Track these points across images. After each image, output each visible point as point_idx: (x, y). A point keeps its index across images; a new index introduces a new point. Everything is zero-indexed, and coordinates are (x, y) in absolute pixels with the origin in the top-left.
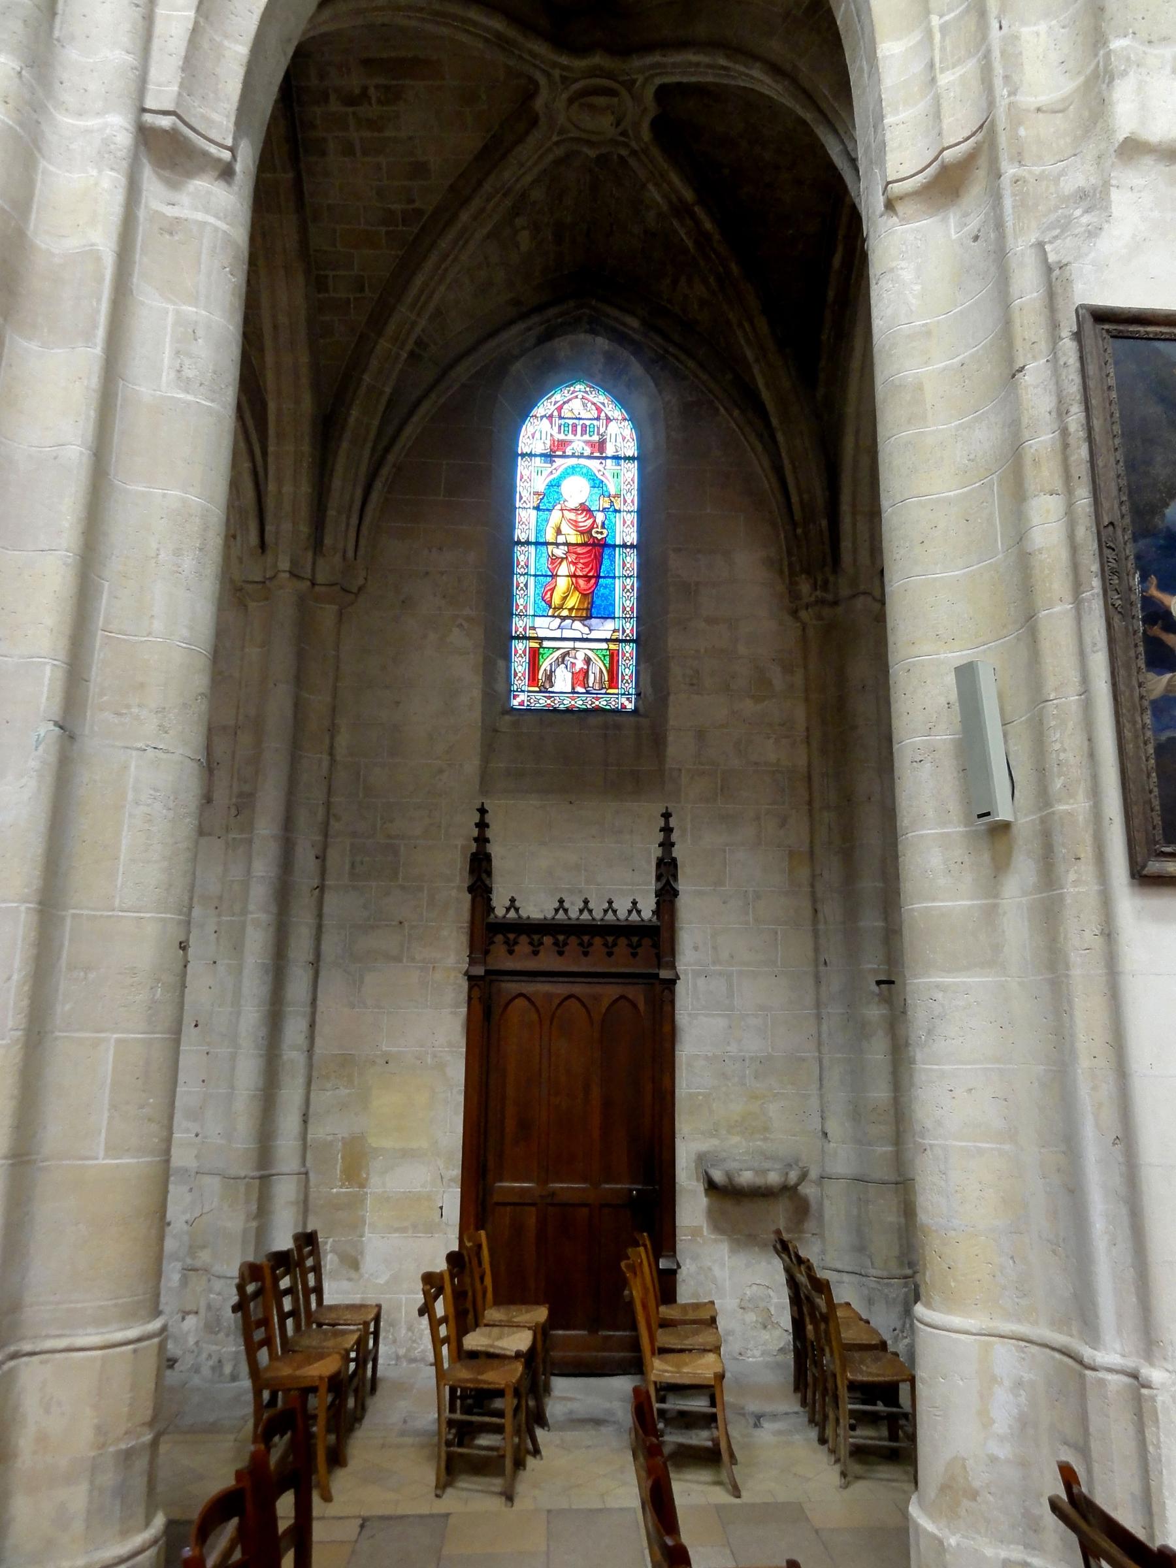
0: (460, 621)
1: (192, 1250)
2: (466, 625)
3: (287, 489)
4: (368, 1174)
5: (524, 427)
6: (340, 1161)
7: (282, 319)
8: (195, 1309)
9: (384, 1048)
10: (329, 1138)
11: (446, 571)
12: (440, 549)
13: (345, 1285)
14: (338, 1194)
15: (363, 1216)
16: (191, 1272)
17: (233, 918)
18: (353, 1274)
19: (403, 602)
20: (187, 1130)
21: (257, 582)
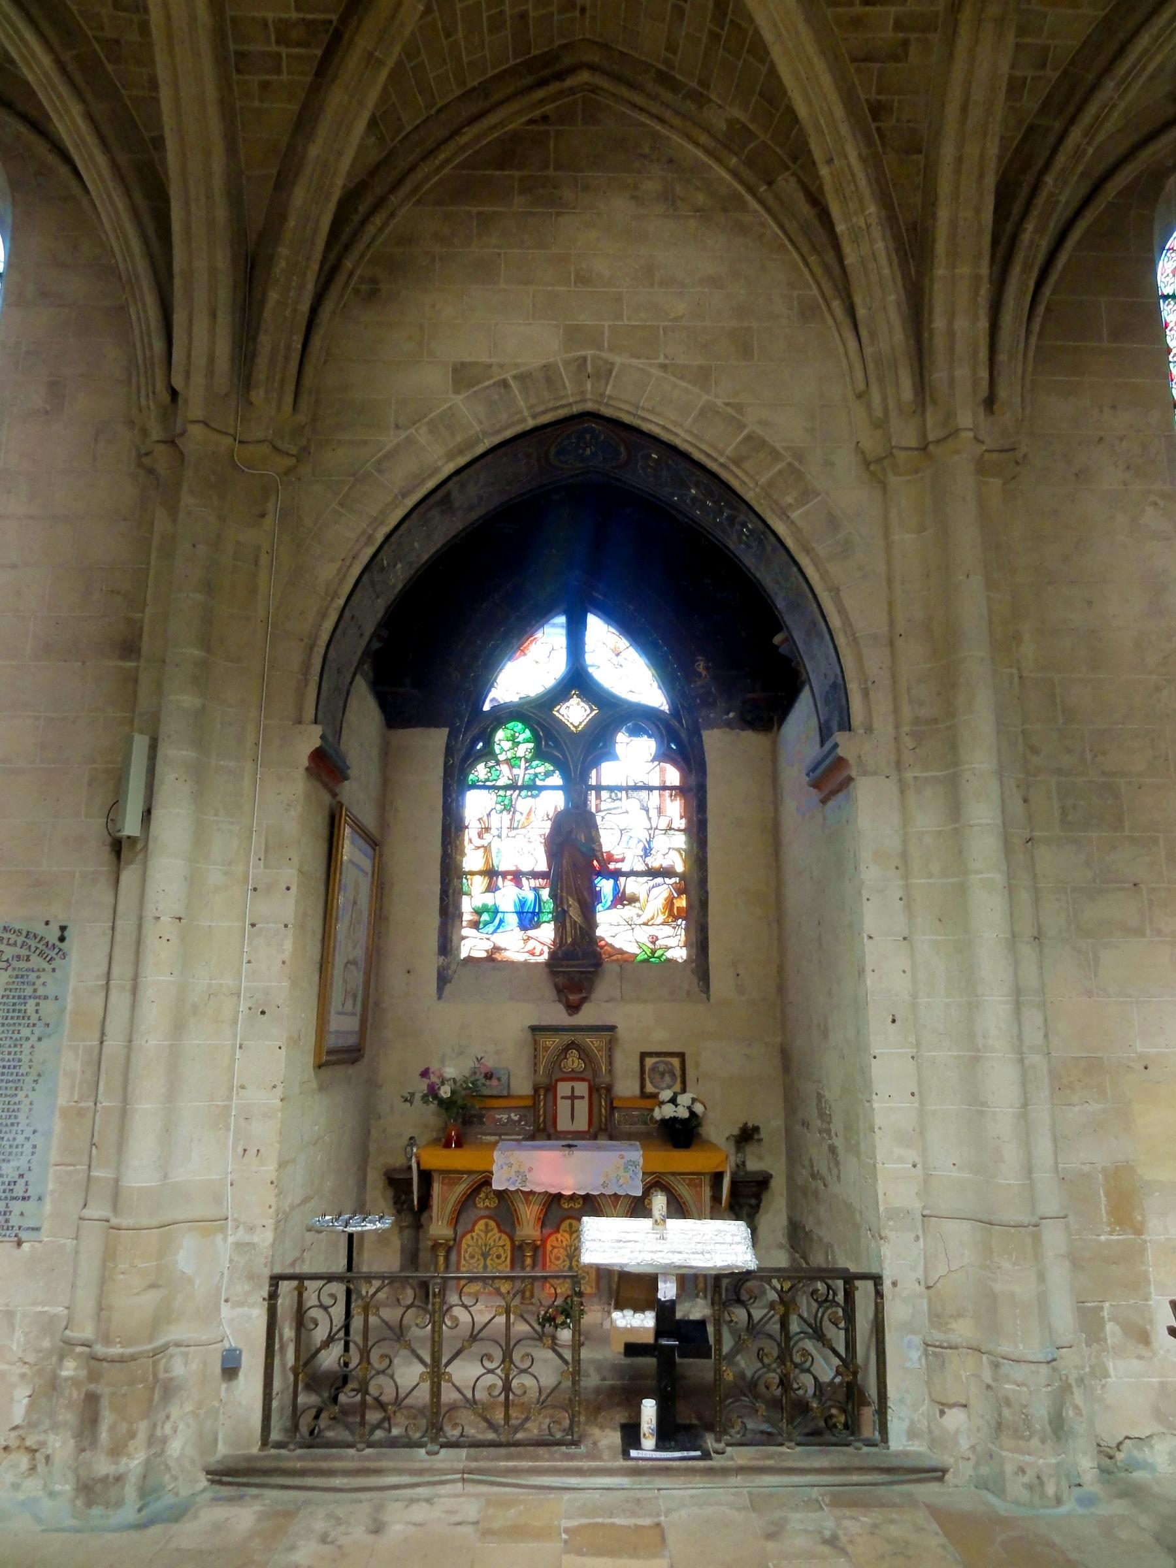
0: (1153, 498)
1: (937, 1318)
2: (1162, 503)
3: (962, 324)
4: (1143, 1216)
5: (1161, 263)
6: (1103, 1199)
7: (978, 95)
8: (964, 1402)
9: (1139, 1049)
10: (1086, 1168)
11: (1124, 436)
12: (1114, 407)
13: (1136, 1365)
14: (1108, 1242)
15: (1146, 1272)
16: (948, 1351)
17: (929, 881)
18: (1144, 1351)
19: (1077, 475)
20: (901, 1160)
21: (910, 449)
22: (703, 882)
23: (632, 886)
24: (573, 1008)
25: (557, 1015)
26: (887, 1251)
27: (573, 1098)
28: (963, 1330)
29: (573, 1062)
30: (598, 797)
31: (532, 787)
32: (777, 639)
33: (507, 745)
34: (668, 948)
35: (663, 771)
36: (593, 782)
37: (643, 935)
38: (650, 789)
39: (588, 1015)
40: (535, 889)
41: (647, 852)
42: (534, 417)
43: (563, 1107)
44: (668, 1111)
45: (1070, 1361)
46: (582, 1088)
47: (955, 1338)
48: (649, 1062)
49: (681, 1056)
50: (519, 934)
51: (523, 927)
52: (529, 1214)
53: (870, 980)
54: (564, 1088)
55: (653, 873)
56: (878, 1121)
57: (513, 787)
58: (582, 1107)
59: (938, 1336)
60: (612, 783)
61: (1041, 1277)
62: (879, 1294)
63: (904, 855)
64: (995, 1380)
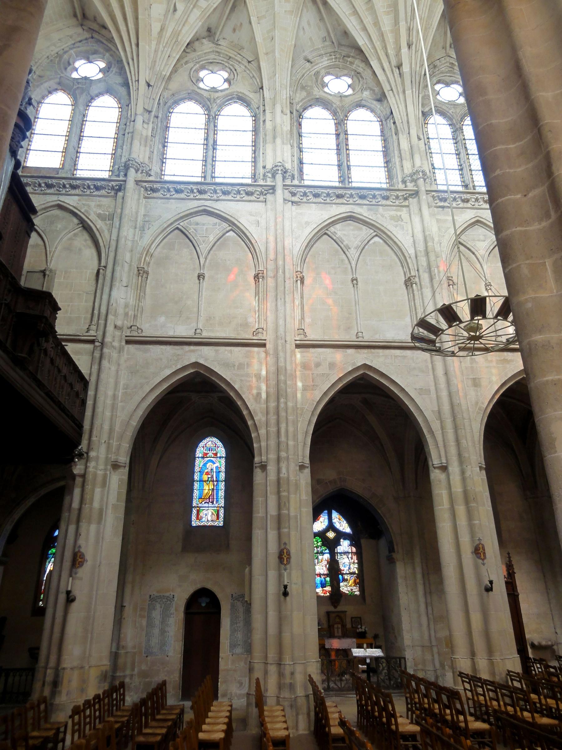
1: (416, 665)
22: (363, 576)
23: (346, 577)
24: (335, 607)
25: (331, 609)
26: (406, 653)
27: (338, 628)
28: (420, 667)
29: (338, 620)
30: (337, 555)
31: (322, 553)
32: (379, 527)
33: (316, 543)
34: (355, 592)
35: (352, 549)
36: (336, 551)
37: (349, 589)
38: (349, 553)
39: (339, 608)
40: (325, 578)
41: (349, 568)
42: (332, 489)
43: (336, 630)
44: (360, 630)
45: (439, 672)
46: (340, 626)
47: (419, 668)
48: (353, 620)
49: (360, 618)
50: (321, 589)
51: (322, 587)
52: (333, 653)
53: (401, 601)
54: (336, 626)
55: (351, 574)
56: (403, 628)
57: (318, 553)
58: (340, 630)
59: (416, 668)
60: (340, 552)
61: (433, 656)
62: (405, 661)
63: (406, 577)
64: (426, 674)
